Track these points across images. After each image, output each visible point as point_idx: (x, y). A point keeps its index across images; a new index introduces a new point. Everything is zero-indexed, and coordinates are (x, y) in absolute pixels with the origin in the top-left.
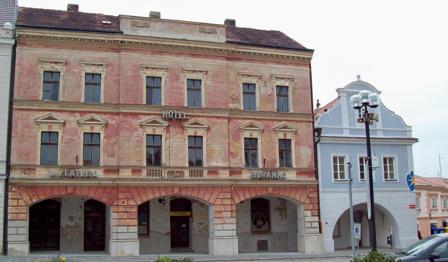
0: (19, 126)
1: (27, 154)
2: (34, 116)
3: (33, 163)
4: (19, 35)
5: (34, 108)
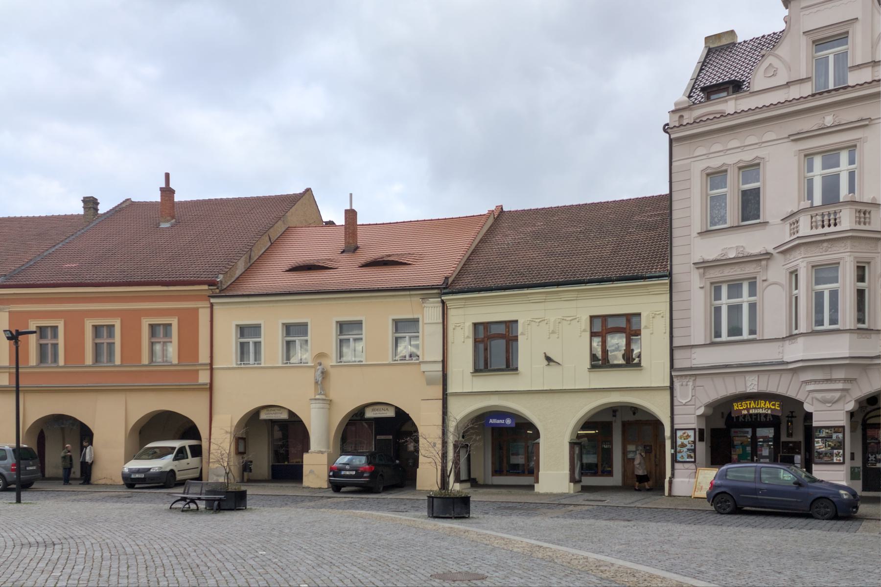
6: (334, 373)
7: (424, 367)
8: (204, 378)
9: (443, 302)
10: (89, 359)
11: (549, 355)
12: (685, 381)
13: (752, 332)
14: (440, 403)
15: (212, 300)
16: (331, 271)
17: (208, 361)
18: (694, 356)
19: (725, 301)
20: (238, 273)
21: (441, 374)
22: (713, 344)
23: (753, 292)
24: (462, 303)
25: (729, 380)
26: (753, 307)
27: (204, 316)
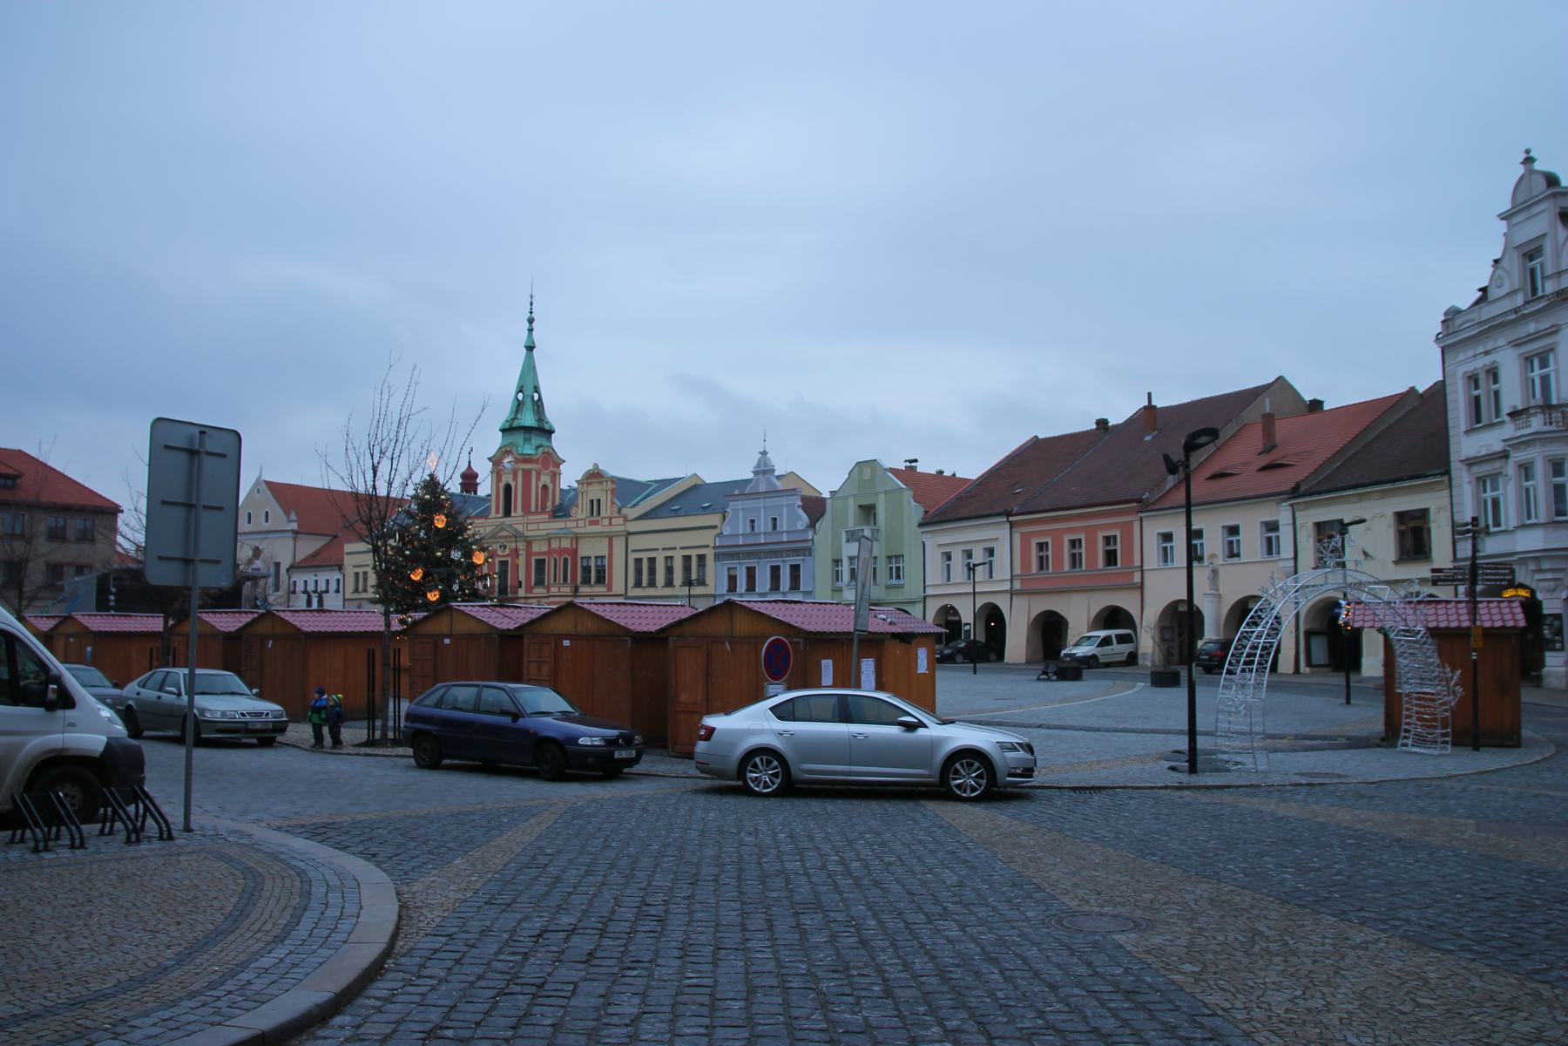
6: (1222, 571)
7: (1281, 564)
8: (1137, 579)
9: (1291, 505)
10: (1067, 566)
11: (1367, 550)
15: (1142, 515)
16: (1233, 478)
17: (1139, 564)
20: (1168, 487)
27: (1136, 525)
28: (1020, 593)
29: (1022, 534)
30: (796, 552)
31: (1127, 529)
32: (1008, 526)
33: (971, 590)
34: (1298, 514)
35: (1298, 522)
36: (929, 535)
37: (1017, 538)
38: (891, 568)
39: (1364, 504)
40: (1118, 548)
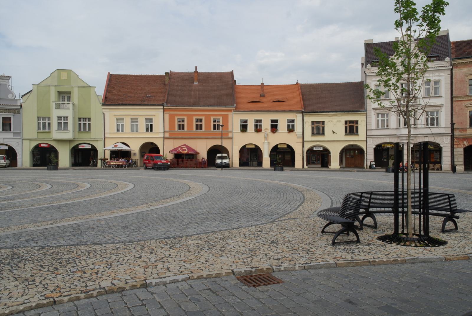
0: (457, 110)
1: (462, 123)
2: (464, 103)
3: (466, 127)
4: (454, 64)
5: (464, 99)
12: (370, 139)
13: (387, 126)
14: (302, 144)
18: (372, 132)
19: (380, 118)
21: (302, 135)
22: (377, 129)
23: (387, 116)
24: (309, 116)
25: (382, 139)
26: (387, 120)
28: (168, 138)
29: (170, 115)
30: (9, 111)
31: (226, 118)
32: (162, 110)
33: (163, 136)
34: (305, 118)
35: (305, 121)
36: (108, 110)
37: (167, 117)
38: (80, 124)
39: (333, 117)
40: (124, 124)
